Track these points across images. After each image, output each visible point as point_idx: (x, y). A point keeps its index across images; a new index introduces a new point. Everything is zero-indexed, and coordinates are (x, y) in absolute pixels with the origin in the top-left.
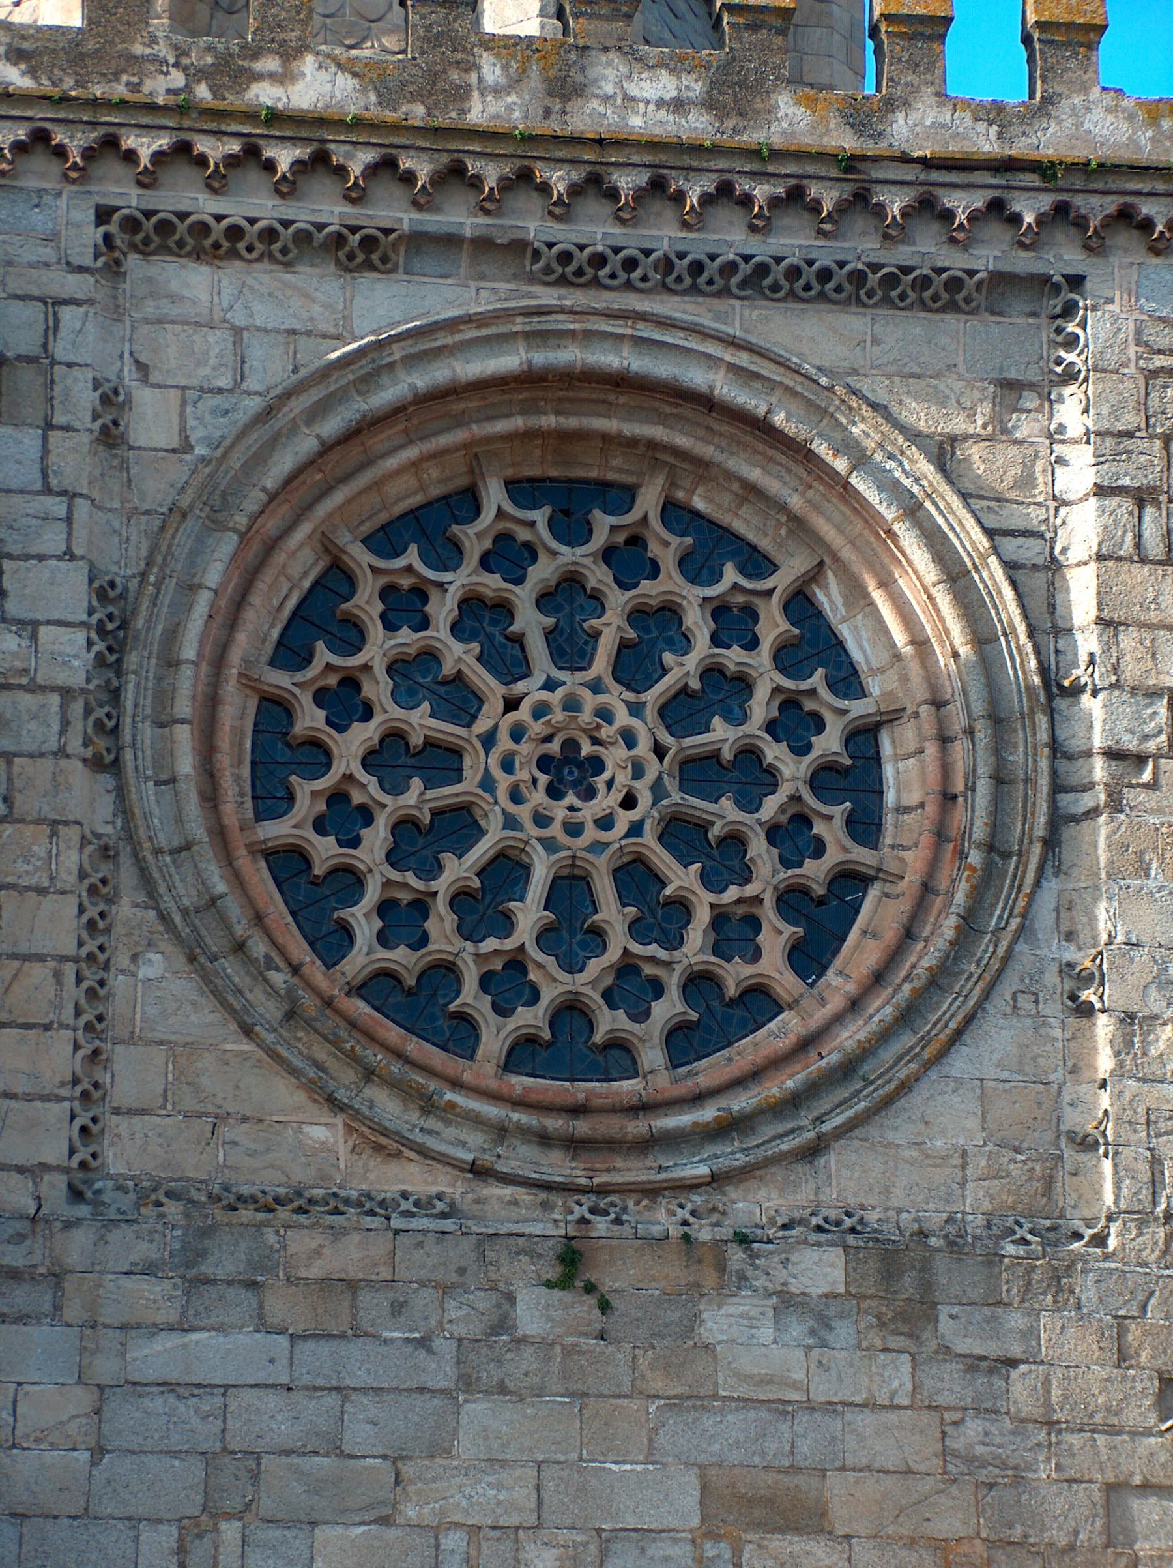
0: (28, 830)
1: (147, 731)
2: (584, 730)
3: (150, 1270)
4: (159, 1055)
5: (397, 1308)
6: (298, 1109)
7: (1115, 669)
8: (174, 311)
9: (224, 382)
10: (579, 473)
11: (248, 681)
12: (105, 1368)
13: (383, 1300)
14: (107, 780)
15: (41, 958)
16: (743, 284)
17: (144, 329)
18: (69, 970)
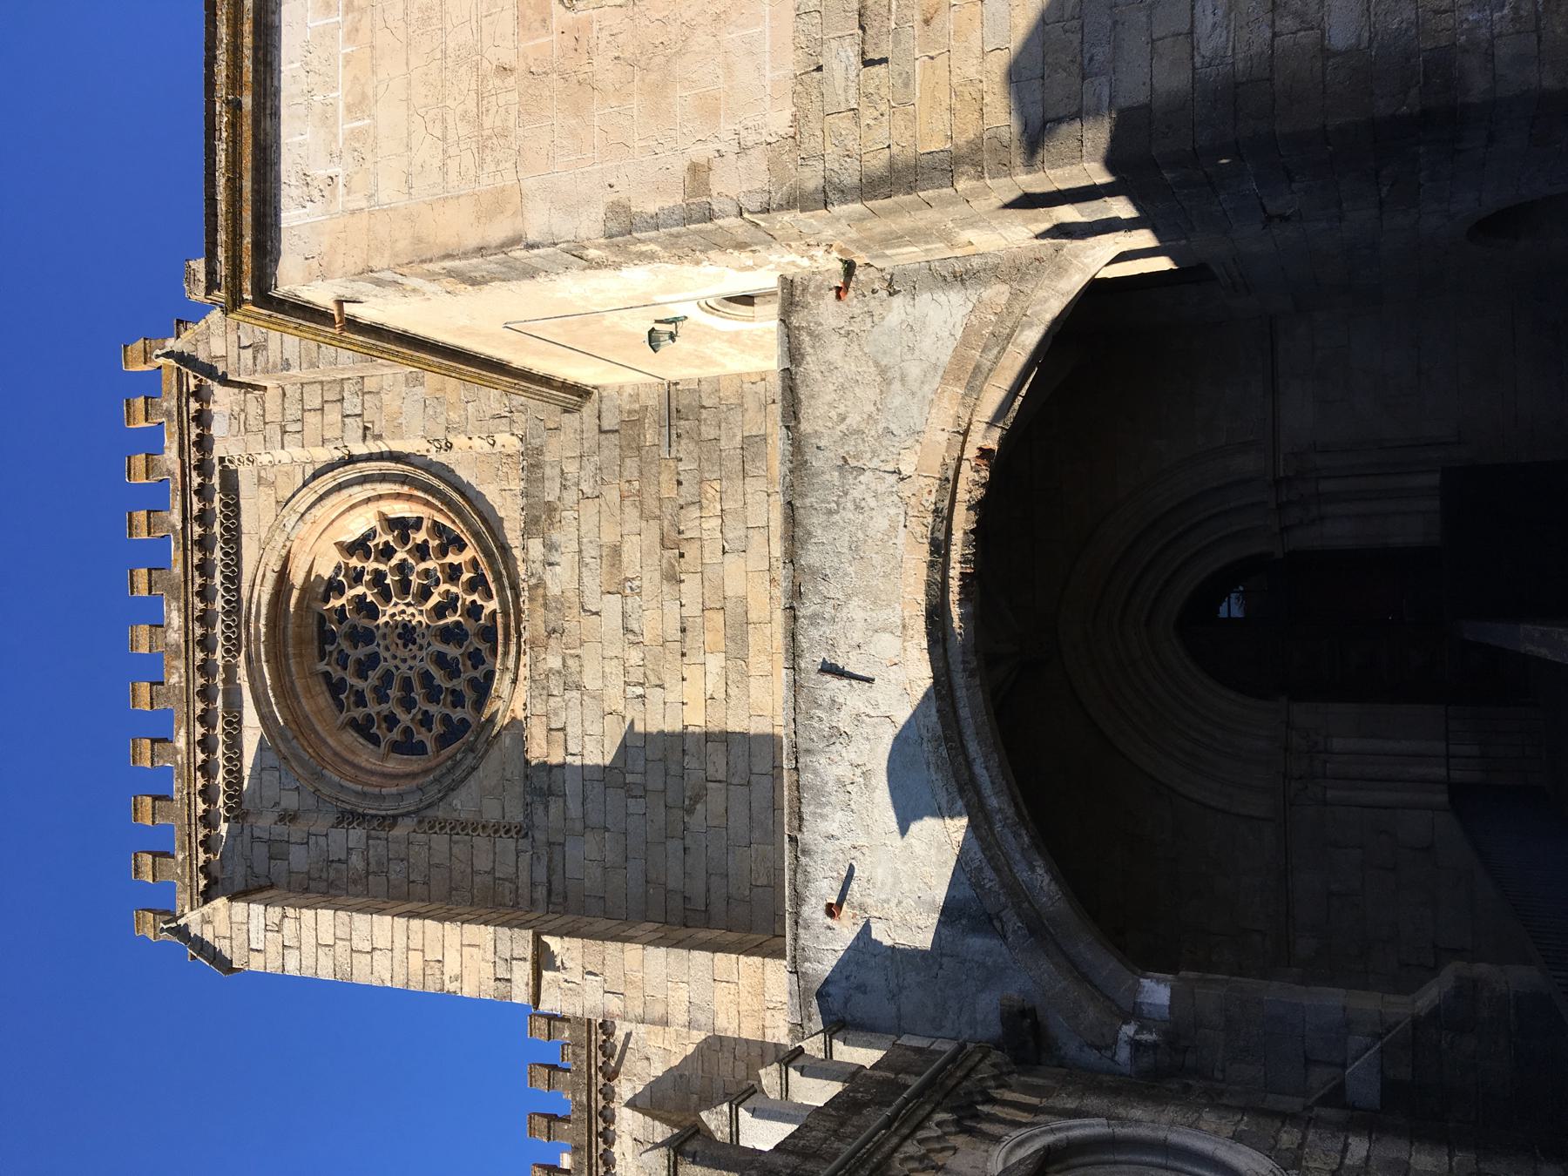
0: (411, 853)
1: (385, 805)
2: (393, 632)
3: (547, 807)
4: (485, 801)
5: (556, 714)
6: (500, 750)
7: (337, 439)
8: (257, 795)
9: (277, 774)
10: (315, 634)
11: (384, 758)
12: (579, 826)
13: (553, 718)
14: (400, 819)
15: (451, 848)
16: (233, 584)
17: (264, 802)
18: (455, 838)
